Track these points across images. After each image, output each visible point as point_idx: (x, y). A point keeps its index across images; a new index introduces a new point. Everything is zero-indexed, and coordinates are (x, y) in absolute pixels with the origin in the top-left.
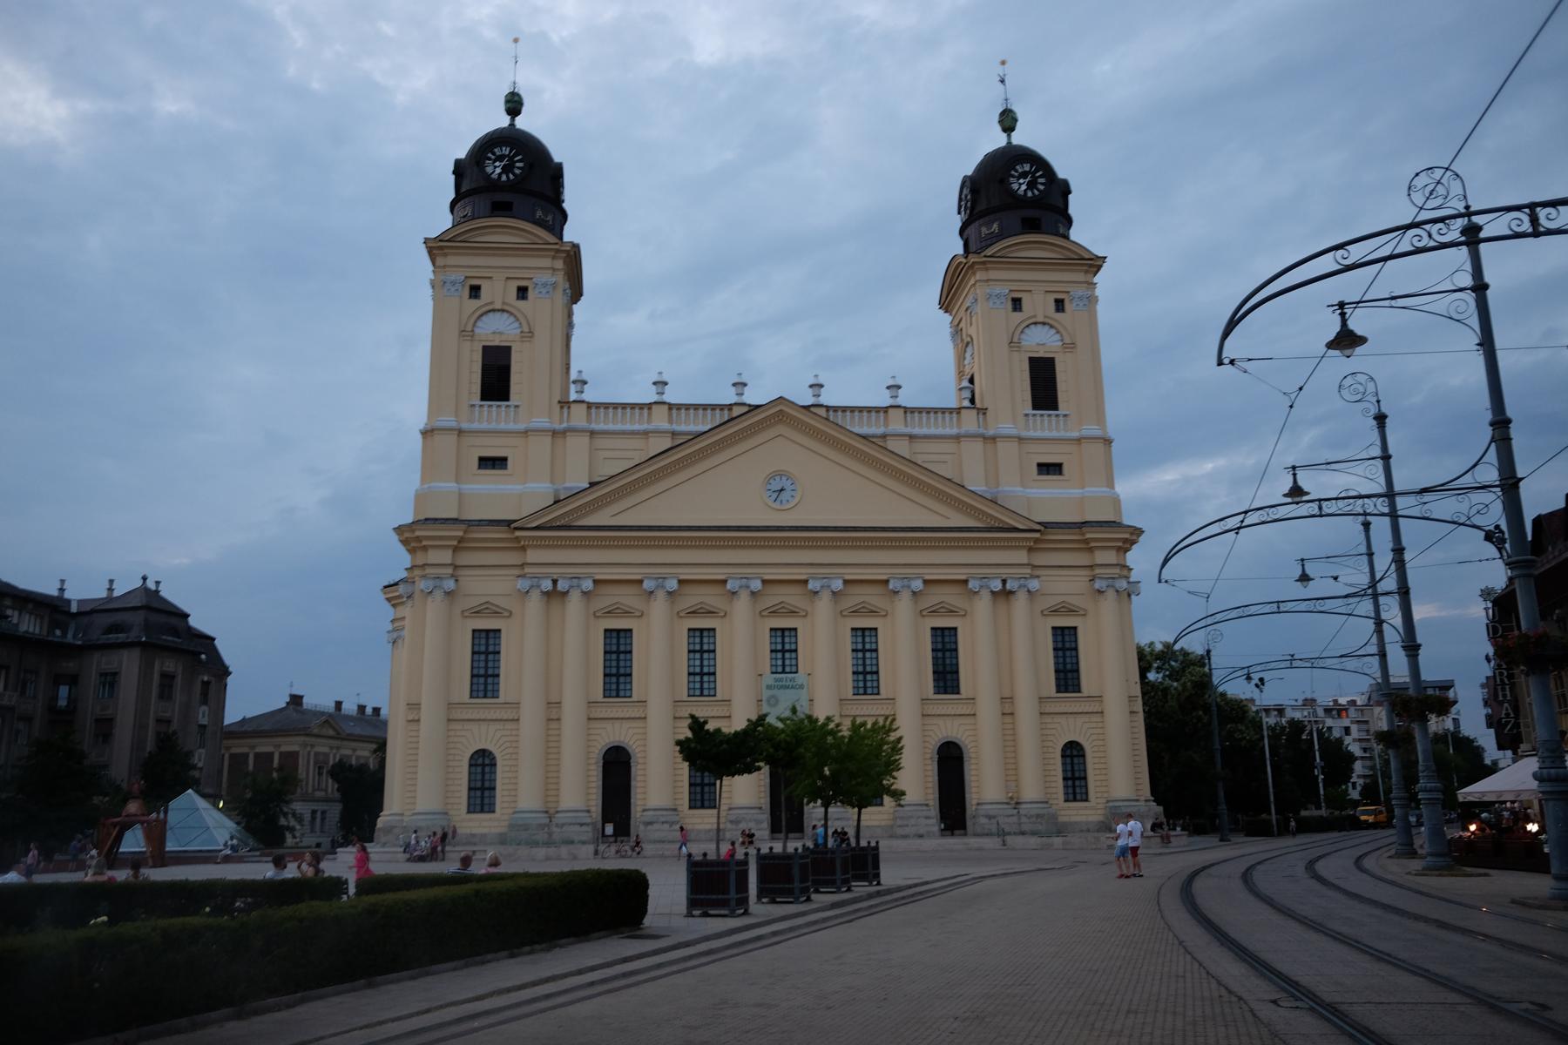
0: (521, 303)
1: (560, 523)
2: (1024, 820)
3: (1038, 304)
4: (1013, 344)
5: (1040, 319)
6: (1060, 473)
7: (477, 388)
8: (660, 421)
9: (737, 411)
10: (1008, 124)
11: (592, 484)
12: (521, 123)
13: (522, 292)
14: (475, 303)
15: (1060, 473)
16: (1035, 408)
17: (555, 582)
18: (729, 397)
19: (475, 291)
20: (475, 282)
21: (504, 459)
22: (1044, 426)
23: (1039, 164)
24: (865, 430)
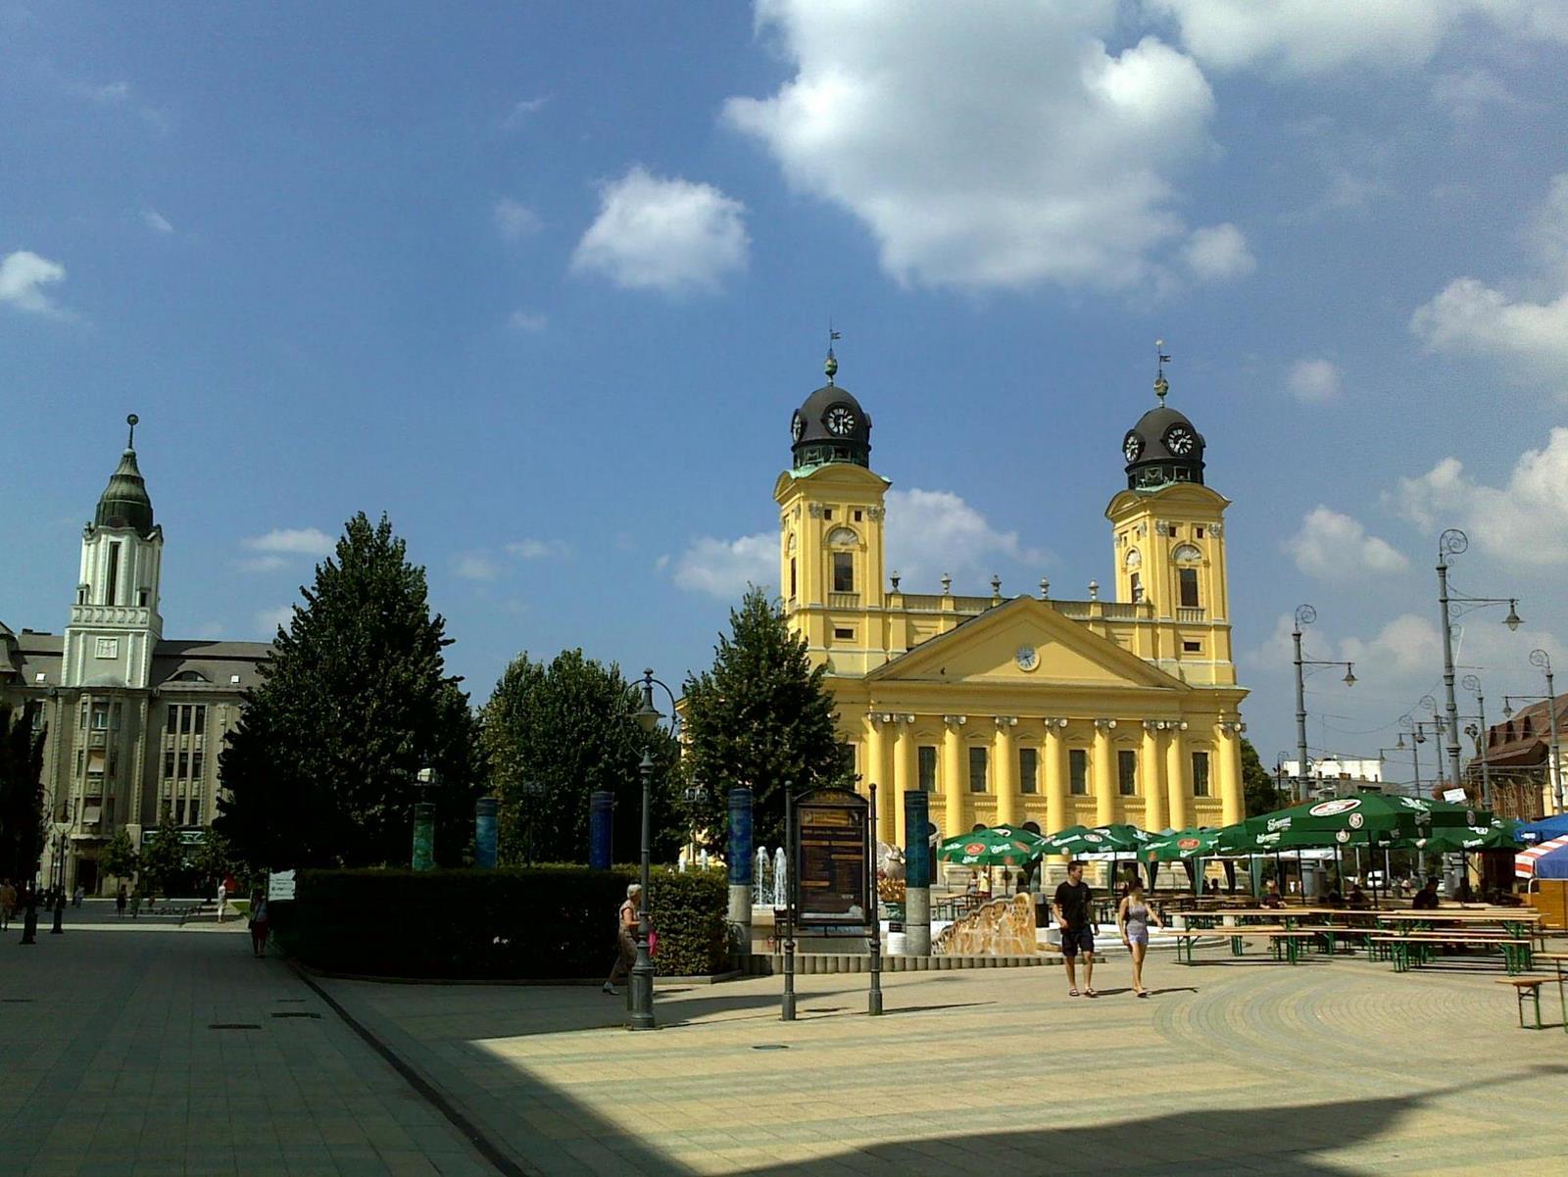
0: (858, 524)
1: (886, 676)
2: (1176, 876)
3: (1184, 533)
4: (1172, 560)
5: (1188, 543)
6: (1198, 650)
7: (832, 583)
8: (947, 606)
9: (994, 604)
10: (1161, 391)
11: (909, 649)
12: (840, 381)
13: (858, 517)
14: (828, 525)
15: (1198, 650)
16: (1183, 604)
17: (891, 715)
18: (993, 595)
19: (828, 515)
20: (828, 508)
21: (851, 631)
22: (1187, 618)
23: (1188, 428)
24: (1076, 617)
